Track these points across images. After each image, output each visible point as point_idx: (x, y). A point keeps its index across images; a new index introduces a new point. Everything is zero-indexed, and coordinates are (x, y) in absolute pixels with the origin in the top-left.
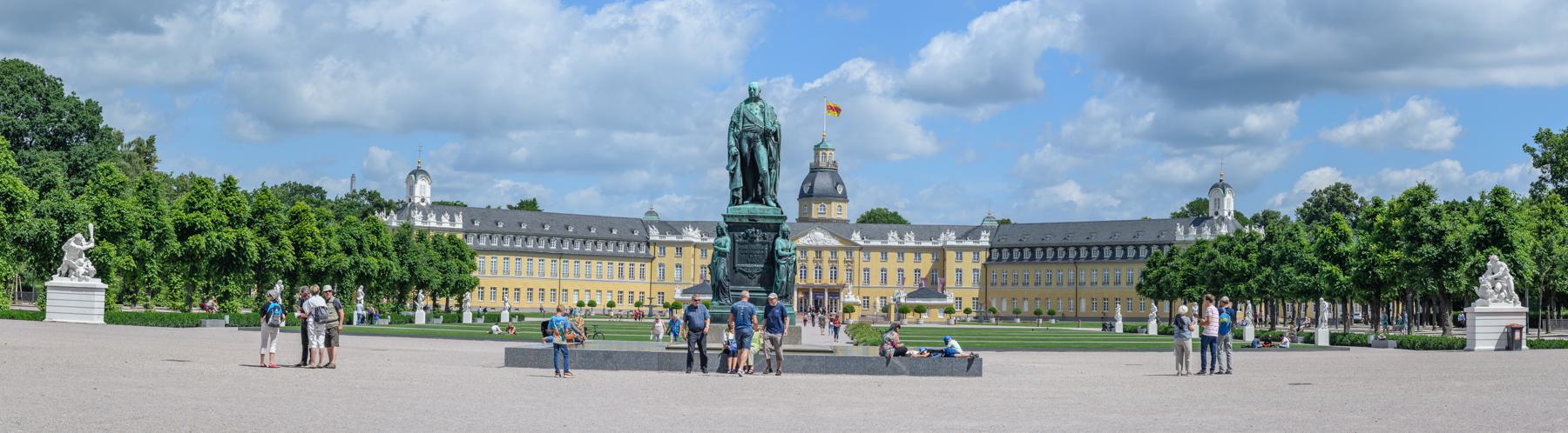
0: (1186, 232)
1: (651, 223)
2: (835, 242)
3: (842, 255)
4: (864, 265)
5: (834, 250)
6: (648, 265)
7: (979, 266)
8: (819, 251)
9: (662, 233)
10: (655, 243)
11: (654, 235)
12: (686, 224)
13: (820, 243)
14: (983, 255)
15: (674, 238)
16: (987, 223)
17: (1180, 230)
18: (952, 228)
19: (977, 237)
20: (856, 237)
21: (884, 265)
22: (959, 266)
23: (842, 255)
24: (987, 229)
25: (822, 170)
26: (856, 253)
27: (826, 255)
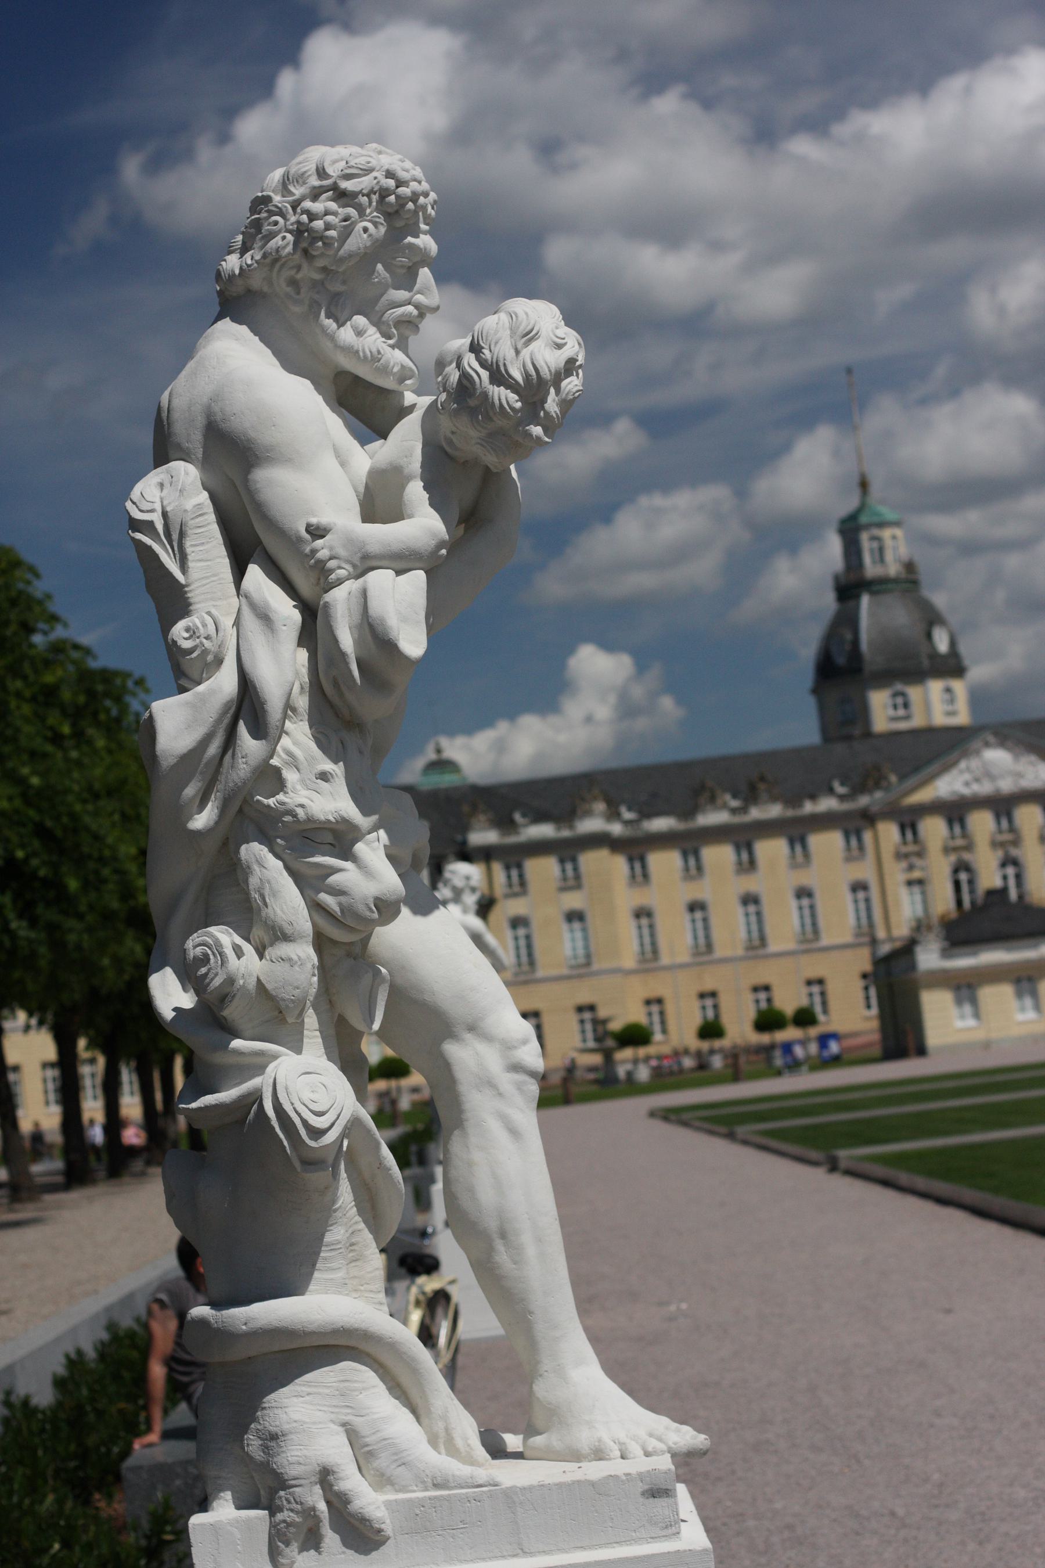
8: (1002, 806)
13: (1006, 786)
25: (878, 586)
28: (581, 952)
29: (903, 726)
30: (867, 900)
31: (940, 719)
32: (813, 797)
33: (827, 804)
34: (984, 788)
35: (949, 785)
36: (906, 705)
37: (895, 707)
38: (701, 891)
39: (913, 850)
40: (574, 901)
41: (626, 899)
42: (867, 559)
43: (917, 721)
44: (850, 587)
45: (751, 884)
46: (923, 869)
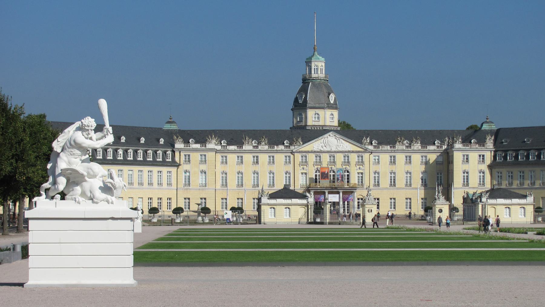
3: (354, 158)
4: (374, 168)
5: (346, 153)
6: (173, 170)
7: (484, 167)
9: (186, 142)
10: (180, 151)
14: (489, 157)
15: (198, 146)
21: (408, 168)
22: (466, 167)
24: (490, 132)
26: (366, 156)
27: (340, 158)
28: (204, 182)
29: (316, 124)
30: (290, 177)
31: (328, 123)
32: (277, 145)
33: (281, 147)
36: (318, 118)
37: (315, 117)
38: (242, 168)
39: (305, 163)
40: (203, 167)
41: (220, 168)
42: (313, 72)
43: (321, 123)
44: (306, 81)
45: (257, 168)
46: (306, 170)
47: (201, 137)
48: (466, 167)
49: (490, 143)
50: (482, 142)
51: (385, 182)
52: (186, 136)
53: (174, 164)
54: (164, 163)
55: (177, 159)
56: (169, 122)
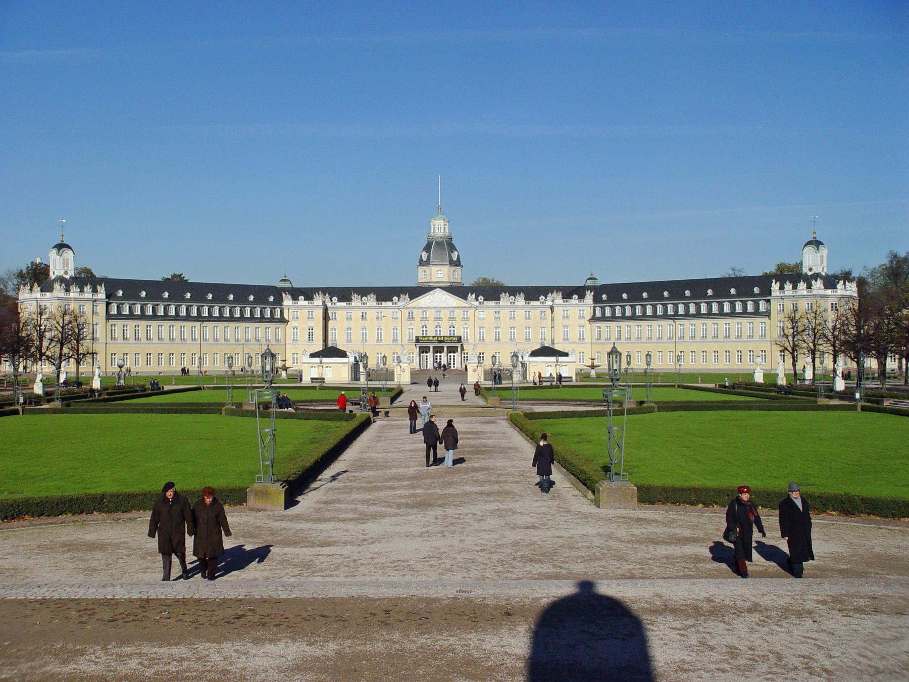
0: (782, 288)
1: (284, 290)
2: (453, 301)
3: (458, 313)
6: (282, 326)
8: (438, 309)
9: (295, 298)
11: (287, 301)
12: (316, 290)
14: (588, 314)
15: (306, 303)
16: (589, 283)
17: (775, 286)
18: (558, 289)
19: (582, 297)
20: (471, 297)
23: (458, 313)
24: (591, 288)
26: (471, 311)
27: (445, 314)
33: (389, 304)
34: (432, 305)
35: (423, 301)
39: (411, 317)
47: (309, 294)
48: (566, 322)
49: (589, 296)
50: (582, 297)
51: (490, 337)
52: (295, 293)
53: (282, 320)
54: (272, 320)
55: (286, 316)
56: (283, 280)
